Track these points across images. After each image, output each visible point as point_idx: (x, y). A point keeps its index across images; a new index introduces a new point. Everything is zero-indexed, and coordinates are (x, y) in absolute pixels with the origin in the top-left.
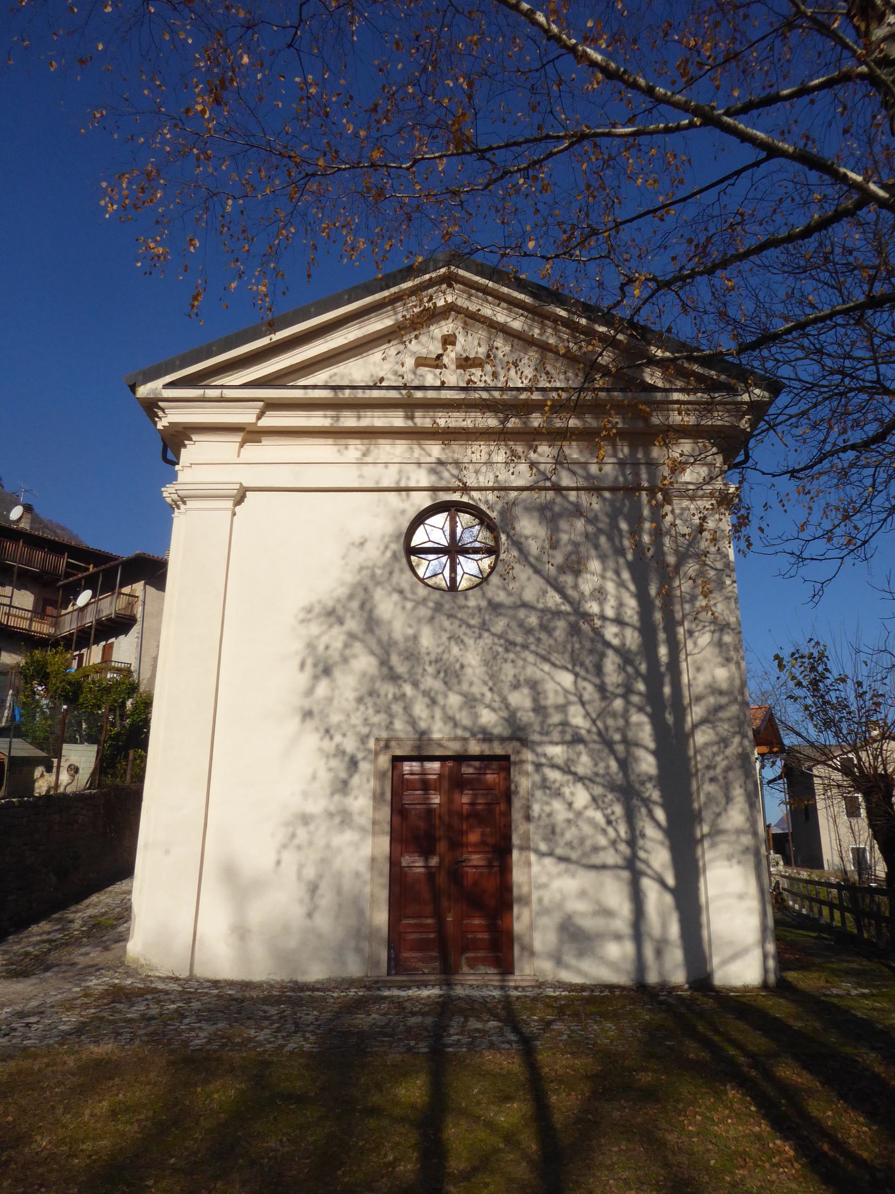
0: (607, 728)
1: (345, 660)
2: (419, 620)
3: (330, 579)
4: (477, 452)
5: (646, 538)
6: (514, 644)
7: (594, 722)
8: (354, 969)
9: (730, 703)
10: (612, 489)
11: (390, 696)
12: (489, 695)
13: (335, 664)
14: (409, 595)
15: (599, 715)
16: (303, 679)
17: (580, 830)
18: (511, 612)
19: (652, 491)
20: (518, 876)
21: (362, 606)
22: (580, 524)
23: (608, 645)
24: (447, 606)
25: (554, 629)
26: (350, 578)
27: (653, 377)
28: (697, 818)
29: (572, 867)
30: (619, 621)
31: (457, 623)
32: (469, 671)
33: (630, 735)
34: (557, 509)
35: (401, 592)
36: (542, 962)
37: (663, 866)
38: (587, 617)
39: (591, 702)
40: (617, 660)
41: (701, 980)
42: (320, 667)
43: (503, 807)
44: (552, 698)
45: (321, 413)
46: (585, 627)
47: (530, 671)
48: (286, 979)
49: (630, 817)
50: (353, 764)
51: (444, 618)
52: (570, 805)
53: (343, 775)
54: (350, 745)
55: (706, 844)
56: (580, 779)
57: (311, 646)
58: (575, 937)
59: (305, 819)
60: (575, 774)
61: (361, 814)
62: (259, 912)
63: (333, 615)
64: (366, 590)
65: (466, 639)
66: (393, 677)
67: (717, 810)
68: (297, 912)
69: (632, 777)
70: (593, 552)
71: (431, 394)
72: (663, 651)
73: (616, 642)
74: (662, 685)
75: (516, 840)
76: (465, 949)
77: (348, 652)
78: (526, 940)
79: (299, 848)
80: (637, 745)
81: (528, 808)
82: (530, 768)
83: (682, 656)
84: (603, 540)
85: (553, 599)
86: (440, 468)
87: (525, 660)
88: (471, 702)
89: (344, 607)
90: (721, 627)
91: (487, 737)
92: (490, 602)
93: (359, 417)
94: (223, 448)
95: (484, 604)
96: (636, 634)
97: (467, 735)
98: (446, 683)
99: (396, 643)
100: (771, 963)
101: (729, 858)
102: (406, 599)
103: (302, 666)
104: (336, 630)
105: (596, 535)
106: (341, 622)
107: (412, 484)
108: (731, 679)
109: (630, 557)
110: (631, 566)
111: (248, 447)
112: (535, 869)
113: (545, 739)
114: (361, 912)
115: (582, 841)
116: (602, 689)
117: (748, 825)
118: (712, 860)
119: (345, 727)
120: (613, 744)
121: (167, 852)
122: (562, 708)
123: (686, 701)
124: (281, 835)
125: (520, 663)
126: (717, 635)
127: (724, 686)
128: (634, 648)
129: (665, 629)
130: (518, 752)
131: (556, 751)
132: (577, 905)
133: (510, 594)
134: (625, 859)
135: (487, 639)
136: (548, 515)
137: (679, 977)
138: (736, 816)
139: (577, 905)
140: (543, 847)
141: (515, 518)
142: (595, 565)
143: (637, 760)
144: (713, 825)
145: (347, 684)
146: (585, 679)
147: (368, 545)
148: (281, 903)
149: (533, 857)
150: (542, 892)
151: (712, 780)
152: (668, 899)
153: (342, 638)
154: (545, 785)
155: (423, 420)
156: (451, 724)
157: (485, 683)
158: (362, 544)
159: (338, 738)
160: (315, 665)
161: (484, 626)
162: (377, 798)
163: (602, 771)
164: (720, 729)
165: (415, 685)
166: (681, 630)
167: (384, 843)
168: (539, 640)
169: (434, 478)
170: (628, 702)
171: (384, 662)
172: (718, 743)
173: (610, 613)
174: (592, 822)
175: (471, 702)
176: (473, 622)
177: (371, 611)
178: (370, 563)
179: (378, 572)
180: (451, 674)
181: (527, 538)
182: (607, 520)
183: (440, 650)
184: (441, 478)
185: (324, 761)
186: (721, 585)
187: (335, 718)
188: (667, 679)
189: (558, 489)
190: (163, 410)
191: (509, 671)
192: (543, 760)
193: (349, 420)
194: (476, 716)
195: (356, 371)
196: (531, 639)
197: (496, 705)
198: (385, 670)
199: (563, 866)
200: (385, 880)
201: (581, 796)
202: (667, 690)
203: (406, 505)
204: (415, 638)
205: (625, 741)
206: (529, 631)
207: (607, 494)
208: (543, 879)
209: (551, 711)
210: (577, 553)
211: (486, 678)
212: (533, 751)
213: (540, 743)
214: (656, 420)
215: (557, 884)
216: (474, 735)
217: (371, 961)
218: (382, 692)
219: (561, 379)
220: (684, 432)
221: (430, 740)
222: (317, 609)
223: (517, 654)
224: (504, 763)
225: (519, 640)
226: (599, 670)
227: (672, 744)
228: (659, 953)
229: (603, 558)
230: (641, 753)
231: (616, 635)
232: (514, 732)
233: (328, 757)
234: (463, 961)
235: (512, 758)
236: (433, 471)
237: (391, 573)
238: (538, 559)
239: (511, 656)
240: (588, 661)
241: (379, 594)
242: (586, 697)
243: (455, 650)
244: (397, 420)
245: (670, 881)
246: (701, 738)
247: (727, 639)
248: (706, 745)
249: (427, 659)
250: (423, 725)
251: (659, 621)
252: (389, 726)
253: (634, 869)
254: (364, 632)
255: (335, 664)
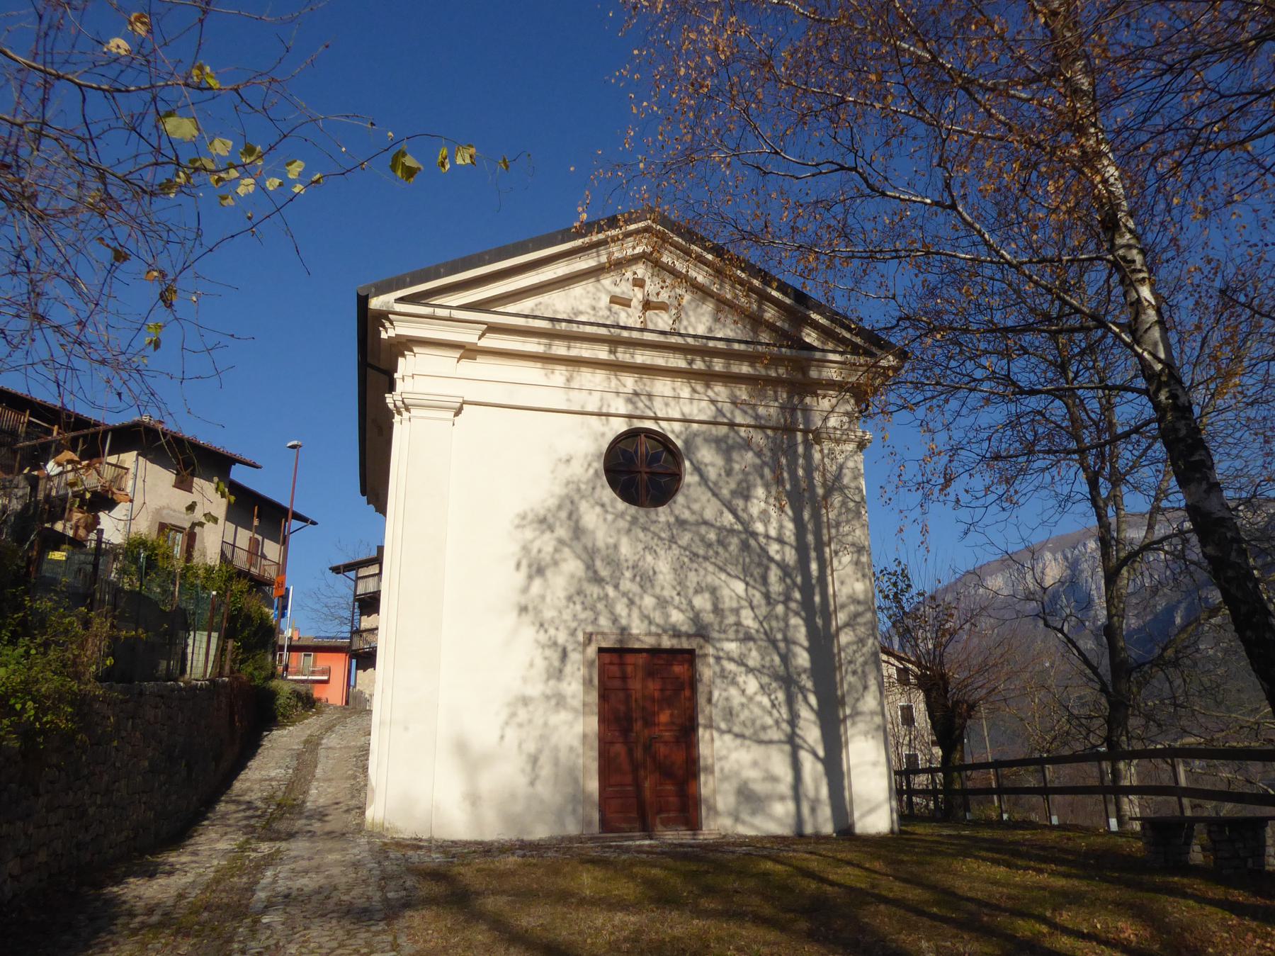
0: (771, 629)
1: (556, 563)
2: (619, 531)
3: (542, 491)
4: (662, 386)
5: (801, 472)
6: (696, 555)
7: (761, 623)
8: (572, 829)
9: (866, 610)
10: (774, 429)
11: (595, 596)
12: (677, 598)
13: (547, 566)
14: (610, 509)
15: (765, 617)
16: (521, 576)
17: (751, 712)
18: (694, 528)
19: (805, 432)
20: (704, 750)
21: (570, 516)
22: (750, 455)
23: (771, 559)
24: (641, 520)
25: (729, 544)
26: (559, 490)
27: (811, 337)
28: (842, 703)
29: (747, 742)
30: (780, 540)
31: (650, 535)
32: (660, 577)
33: (789, 634)
34: (730, 442)
35: (603, 506)
36: (723, 819)
37: (815, 741)
38: (754, 535)
39: (759, 606)
40: (779, 573)
41: (845, 831)
42: (534, 568)
43: (687, 693)
44: (728, 603)
45: (536, 340)
46: (752, 542)
47: (709, 579)
48: (514, 838)
49: (790, 702)
50: (564, 655)
51: (639, 531)
52: (743, 691)
53: (557, 663)
54: (562, 637)
55: (849, 723)
56: (750, 670)
57: (526, 549)
58: (749, 798)
59: (525, 701)
60: (746, 666)
61: (573, 697)
62: (489, 782)
63: (544, 523)
64: (572, 502)
65: (658, 550)
66: (597, 580)
67: (856, 695)
68: (522, 781)
69: (791, 669)
70: (759, 481)
71: (635, 335)
72: (814, 566)
73: (777, 557)
74: (813, 594)
75: (701, 720)
76: (660, 811)
77: (557, 556)
78: (712, 801)
79: (520, 725)
80: (795, 643)
81: (710, 693)
82: (711, 660)
83: (829, 572)
84: (767, 471)
85: (728, 518)
86: (636, 399)
87: (705, 569)
88: (663, 603)
89: (554, 516)
90: (860, 550)
91: (677, 634)
92: (677, 518)
93: (569, 348)
94: (445, 362)
95: (672, 520)
96: (793, 552)
97: (660, 631)
98: (642, 587)
99: (599, 550)
100: (895, 816)
101: (866, 734)
102: (607, 512)
103: (518, 566)
104: (548, 536)
105: (762, 467)
106: (551, 529)
107: (612, 411)
108: (866, 591)
109: (788, 487)
110: (789, 495)
111: (463, 361)
112: (717, 743)
113: (723, 636)
114: (576, 781)
115: (753, 722)
116: (767, 596)
117: (879, 709)
118: (853, 736)
119: (557, 621)
120: (776, 643)
121: (406, 729)
122: (736, 611)
123: (832, 608)
124: (504, 716)
125: (702, 572)
126: (855, 556)
127: (861, 597)
128: (792, 563)
129: (816, 549)
130: (701, 648)
131: (732, 647)
132: (749, 774)
133: (693, 513)
134: (787, 735)
135: (676, 551)
136: (726, 448)
137: (828, 829)
138: (870, 702)
139: (749, 774)
140: (723, 726)
141: (697, 448)
142: (760, 492)
143: (795, 655)
144: (854, 707)
145: (559, 583)
146: (754, 588)
147: (573, 462)
148: (507, 774)
149: (716, 734)
150: (723, 763)
151: (854, 673)
152: (820, 767)
153: (553, 543)
154: (723, 675)
155: (623, 355)
156: (646, 622)
157: (674, 588)
158: (568, 461)
159: (552, 631)
160: (530, 566)
161: (673, 540)
162: (587, 682)
163: (767, 664)
164: (858, 632)
165: (616, 587)
166: (827, 550)
167: (593, 723)
168: (717, 553)
169: (630, 407)
170: (787, 608)
171: (590, 567)
172: (857, 643)
173: (773, 533)
174: (760, 704)
175: (663, 603)
176: (663, 535)
177: (577, 522)
178: (575, 479)
179: (583, 487)
180: (646, 579)
181: (706, 465)
182: (769, 454)
183: (636, 557)
184: (637, 408)
185: (540, 650)
186: (858, 515)
187: (549, 614)
188: (817, 590)
189: (732, 425)
190: (391, 323)
191: (693, 579)
192: (721, 654)
193: (560, 349)
194: (667, 616)
195: (559, 303)
196: (711, 553)
197: (684, 607)
198: (590, 574)
199: (738, 741)
200: (595, 754)
201: (752, 685)
202: (817, 599)
203: (606, 429)
204: (616, 547)
205: (785, 639)
206: (709, 545)
207: (769, 432)
208: (724, 752)
209: (727, 613)
210: (746, 481)
211: (675, 583)
212: (714, 647)
213: (720, 640)
214: (814, 374)
215: (734, 756)
216: (665, 631)
217: (587, 823)
218: (588, 593)
219: (729, 330)
220: (831, 384)
221: (630, 634)
222: (530, 516)
223: (700, 565)
224: (689, 657)
225: (701, 552)
226: (765, 580)
227: (822, 642)
228: (813, 810)
229: (767, 486)
230: (798, 650)
231: (778, 552)
232: (698, 630)
233: (543, 647)
234: (658, 821)
235: (697, 652)
236: (629, 401)
237: (594, 488)
238: (716, 484)
239: (695, 566)
240: (757, 572)
241: (584, 506)
242: (755, 603)
243: (649, 558)
244: (602, 353)
245: (821, 753)
246: (845, 638)
247: (864, 559)
248: (849, 644)
249: (625, 565)
250: (624, 622)
251: (812, 542)
252: (595, 621)
253: (793, 743)
254: (572, 539)
255: (547, 566)
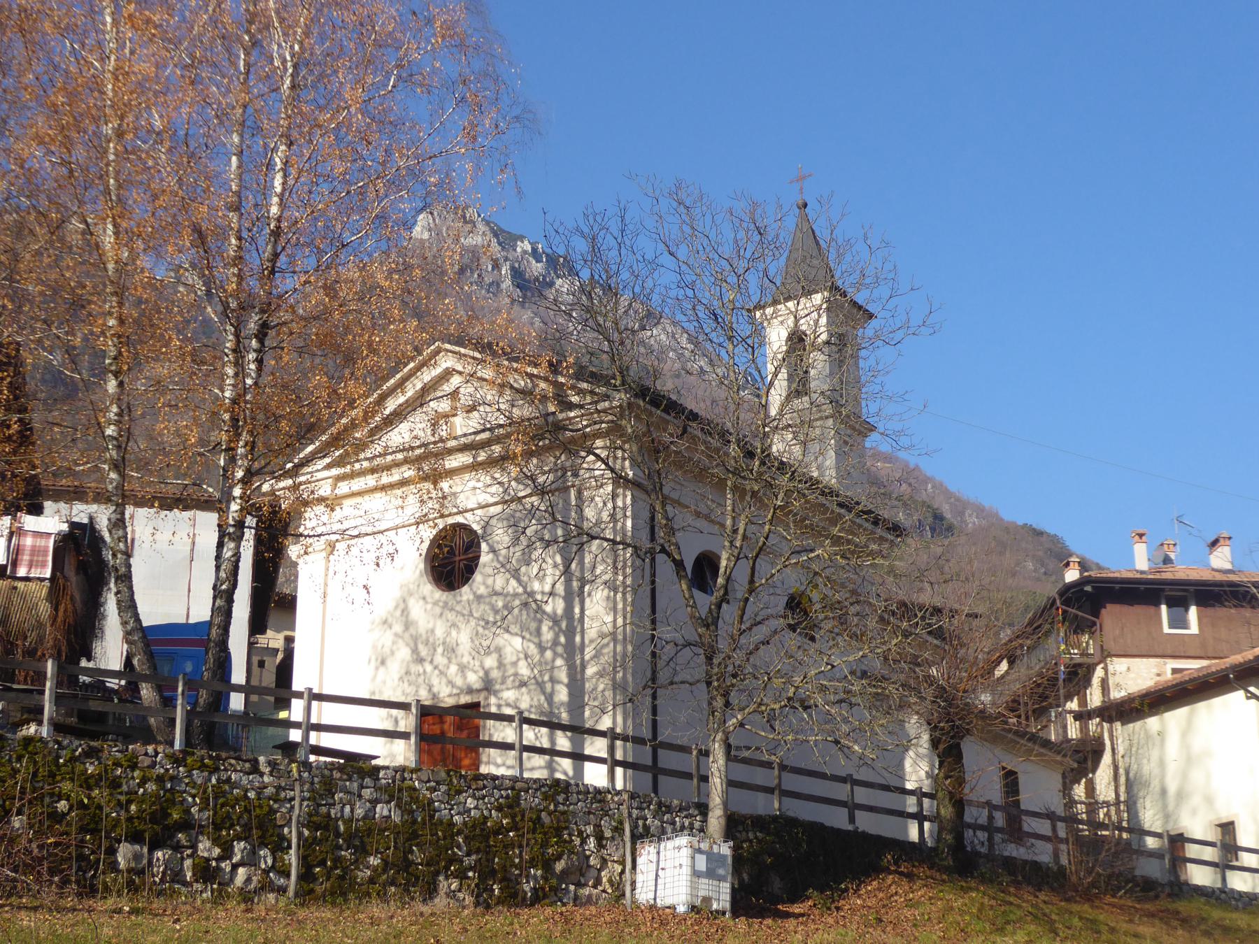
1: (392, 653)
32: (461, 647)
35: (424, 598)
38: (531, 594)
72: (577, 610)
74: (574, 635)
88: (463, 668)
91: (470, 691)
122: (515, 664)
171: (415, 651)
179: (411, 586)
180: (451, 651)
197: (476, 668)
204: (433, 631)
209: (508, 667)
226: (538, 632)
240: (533, 625)
243: (454, 633)
246: (591, 671)
